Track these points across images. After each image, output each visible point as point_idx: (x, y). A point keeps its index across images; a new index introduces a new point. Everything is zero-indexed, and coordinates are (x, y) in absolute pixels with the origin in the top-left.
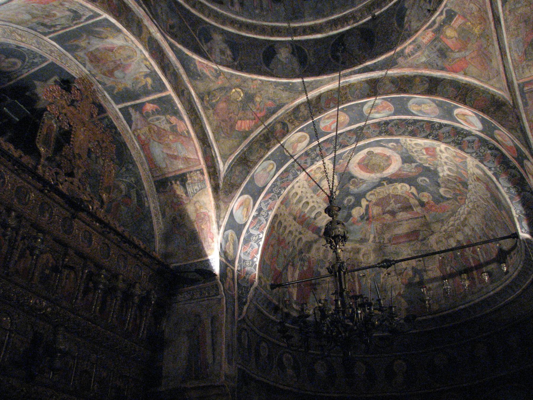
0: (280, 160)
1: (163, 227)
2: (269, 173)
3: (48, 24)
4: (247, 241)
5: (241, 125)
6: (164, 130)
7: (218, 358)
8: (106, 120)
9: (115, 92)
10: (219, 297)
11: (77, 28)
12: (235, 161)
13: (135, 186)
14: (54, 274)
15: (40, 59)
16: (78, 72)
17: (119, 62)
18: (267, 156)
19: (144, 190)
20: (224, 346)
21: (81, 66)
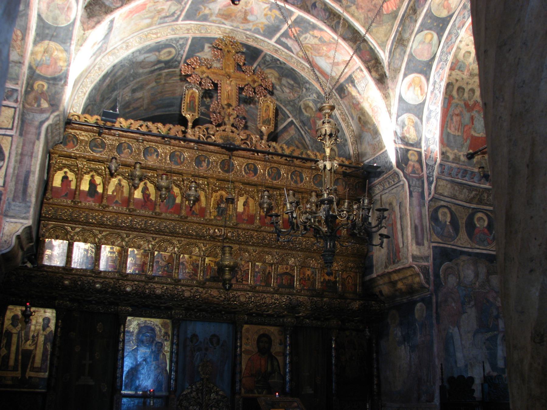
0: (438, 26)
1: (355, 129)
2: (430, 43)
3: (168, 15)
4: (428, 119)
5: (388, 7)
6: (316, 44)
7: (406, 241)
8: (267, 57)
9: (261, 31)
10: (402, 183)
11: (190, 5)
12: (395, 44)
14: (231, 205)
16: (220, 33)
17: (243, 10)
18: (416, 29)
20: (409, 229)
21: (223, 26)
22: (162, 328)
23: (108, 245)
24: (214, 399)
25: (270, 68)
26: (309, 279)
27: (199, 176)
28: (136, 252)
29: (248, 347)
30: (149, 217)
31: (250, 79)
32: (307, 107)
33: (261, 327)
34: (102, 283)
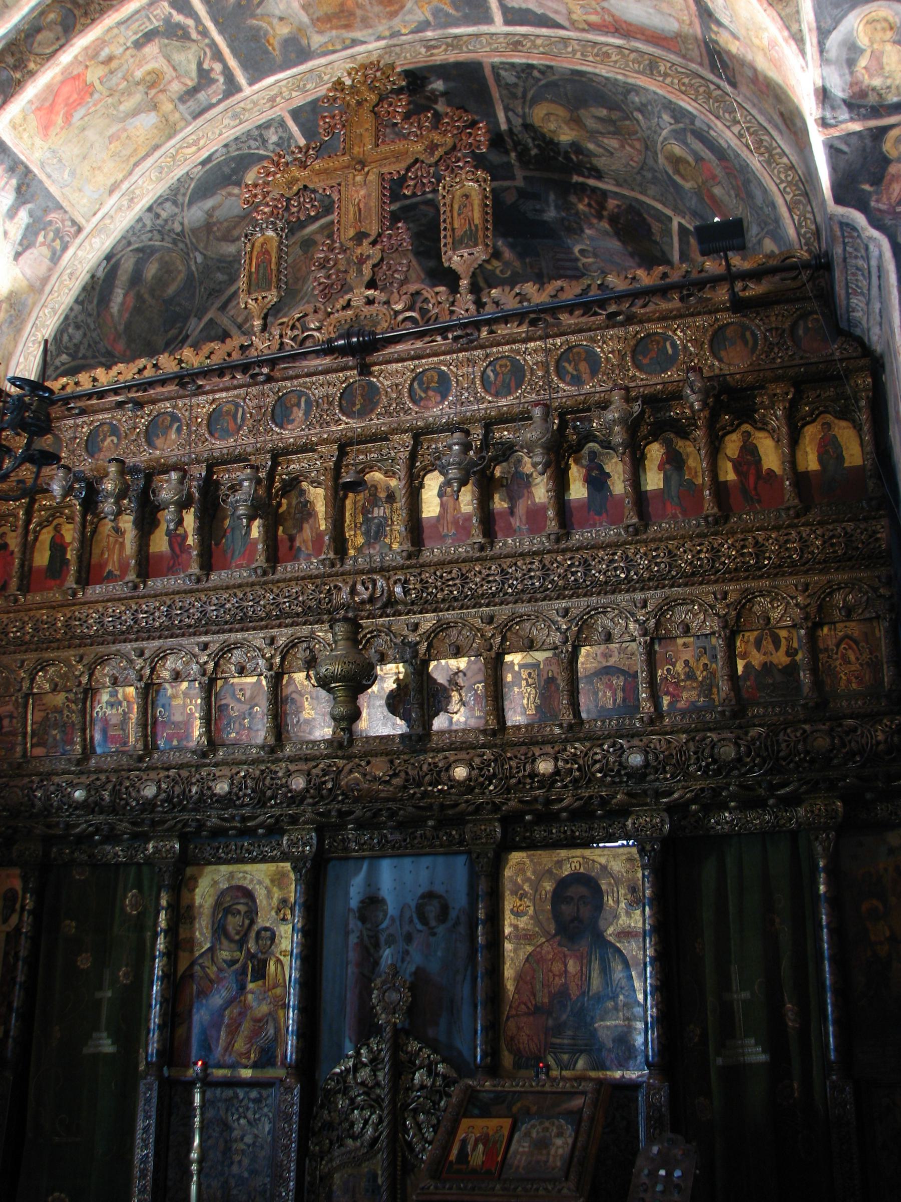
3: (190, 84)
8: (502, 73)
9: (451, 11)
10: (874, 251)
13: (681, 125)
15: (272, 130)
19: (695, 117)
22: (275, 889)
23: (105, 687)
24: (422, 1087)
25: (534, 102)
26: (691, 676)
27: (287, 451)
28: (170, 692)
29: (523, 922)
30: (178, 593)
31: (419, 147)
32: (677, 162)
33: (563, 853)
34: (88, 788)
